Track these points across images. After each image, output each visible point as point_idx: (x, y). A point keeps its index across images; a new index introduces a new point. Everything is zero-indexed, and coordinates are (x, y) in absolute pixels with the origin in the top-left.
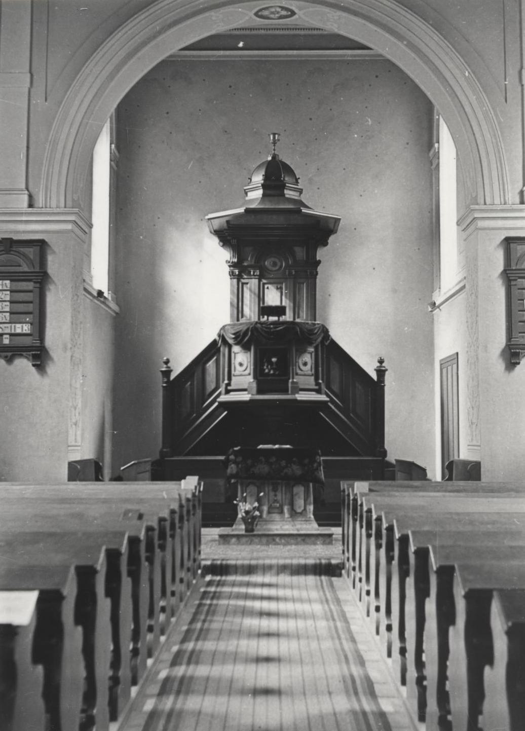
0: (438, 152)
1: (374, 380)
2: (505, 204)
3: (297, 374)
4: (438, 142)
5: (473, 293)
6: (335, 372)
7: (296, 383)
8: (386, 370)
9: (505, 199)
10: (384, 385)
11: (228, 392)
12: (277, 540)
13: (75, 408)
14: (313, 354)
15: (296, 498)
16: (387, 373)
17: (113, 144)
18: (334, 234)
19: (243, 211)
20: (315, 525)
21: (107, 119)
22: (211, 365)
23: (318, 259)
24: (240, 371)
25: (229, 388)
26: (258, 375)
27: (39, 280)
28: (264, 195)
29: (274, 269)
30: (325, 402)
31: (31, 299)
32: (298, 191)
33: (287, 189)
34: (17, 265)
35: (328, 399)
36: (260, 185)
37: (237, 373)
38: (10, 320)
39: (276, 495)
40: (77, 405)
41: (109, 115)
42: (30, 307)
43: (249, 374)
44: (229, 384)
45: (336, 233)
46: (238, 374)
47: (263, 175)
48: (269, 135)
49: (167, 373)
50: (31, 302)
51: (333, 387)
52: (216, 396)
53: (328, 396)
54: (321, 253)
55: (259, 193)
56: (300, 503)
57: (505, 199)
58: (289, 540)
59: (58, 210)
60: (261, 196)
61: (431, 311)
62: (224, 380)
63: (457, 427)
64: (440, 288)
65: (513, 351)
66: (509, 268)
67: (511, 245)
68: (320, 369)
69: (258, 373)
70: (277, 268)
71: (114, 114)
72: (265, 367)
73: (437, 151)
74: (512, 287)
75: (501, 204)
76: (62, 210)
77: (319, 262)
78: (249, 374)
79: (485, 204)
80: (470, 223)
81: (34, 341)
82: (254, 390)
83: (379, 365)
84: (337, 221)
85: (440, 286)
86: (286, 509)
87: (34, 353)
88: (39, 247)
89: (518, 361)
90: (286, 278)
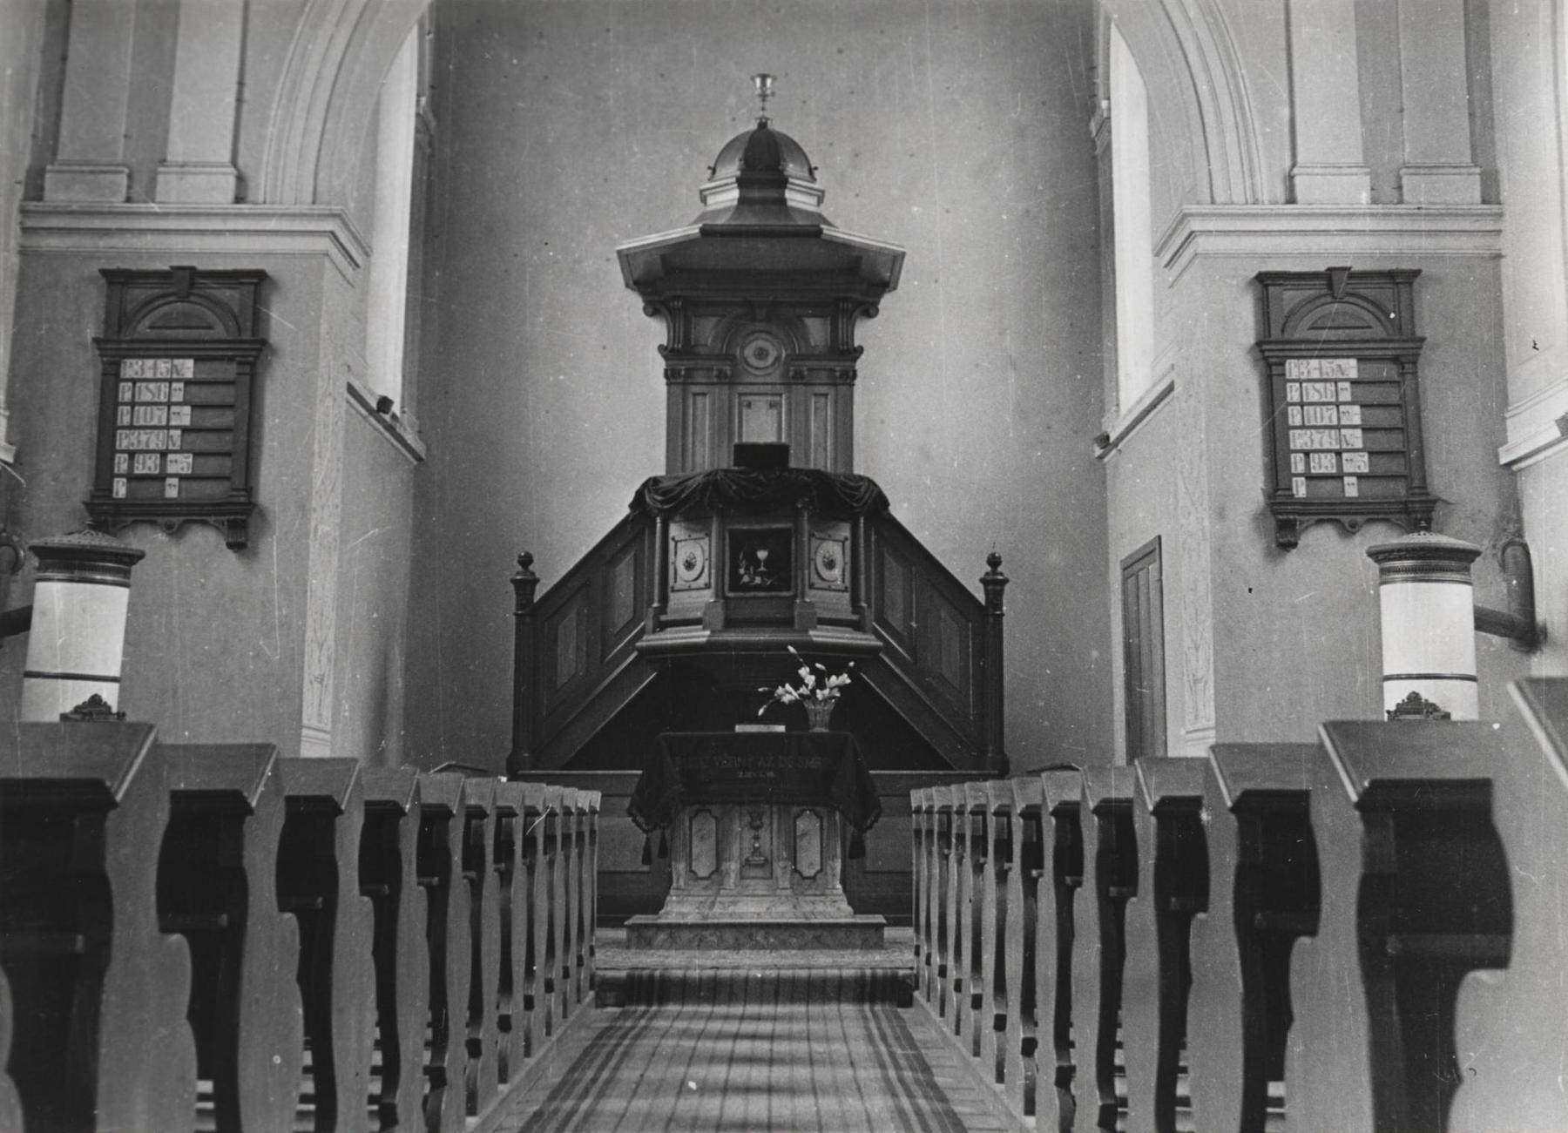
0: (1109, 118)
1: (979, 603)
2: (1256, 202)
3: (812, 586)
4: (1109, 99)
5: (1191, 396)
6: (896, 589)
7: (811, 604)
8: (1006, 581)
9: (1254, 192)
10: (1002, 615)
11: (662, 626)
12: (760, 937)
13: (321, 646)
14: (848, 543)
15: (802, 844)
16: (1007, 587)
17: (423, 95)
18: (890, 291)
19: (697, 231)
20: (846, 907)
21: (411, 28)
22: (624, 574)
23: (857, 344)
24: (687, 581)
25: (663, 618)
26: (726, 587)
27: (251, 359)
28: (742, 201)
29: (761, 364)
30: (875, 650)
31: (229, 400)
32: (815, 195)
33: (791, 189)
34: (205, 325)
35: (880, 644)
36: (734, 180)
37: (680, 584)
38: (182, 446)
39: (756, 838)
40: (326, 640)
41: (416, 17)
42: (227, 418)
43: (707, 586)
44: (663, 609)
45: (895, 288)
46: (682, 588)
47: (740, 160)
48: (753, 79)
49: (525, 585)
50: (231, 407)
51: (890, 619)
52: (634, 636)
53: (879, 637)
54: (864, 332)
55: (734, 195)
56: (810, 859)
57: (1254, 192)
58: (785, 935)
59: (296, 209)
60: (735, 203)
61: (1101, 457)
62: (651, 601)
63: (1157, 603)
64: (1118, 405)
65: (1280, 517)
66: (1267, 339)
67: (1271, 289)
68: (862, 577)
69: (730, 583)
70: (770, 360)
71: (427, 15)
72: (742, 571)
73: (1105, 115)
74: (1275, 378)
75: (1247, 203)
76: (305, 208)
77: (860, 350)
78: (707, 586)
79: (1213, 202)
80: (1181, 247)
81: (234, 493)
82: (719, 625)
83: (989, 569)
84: (897, 259)
85: (1118, 399)
86: (778, 867)
87: (232, 517)
88: (252, 287)
89: (1293, 540)
90: (790, 384)
